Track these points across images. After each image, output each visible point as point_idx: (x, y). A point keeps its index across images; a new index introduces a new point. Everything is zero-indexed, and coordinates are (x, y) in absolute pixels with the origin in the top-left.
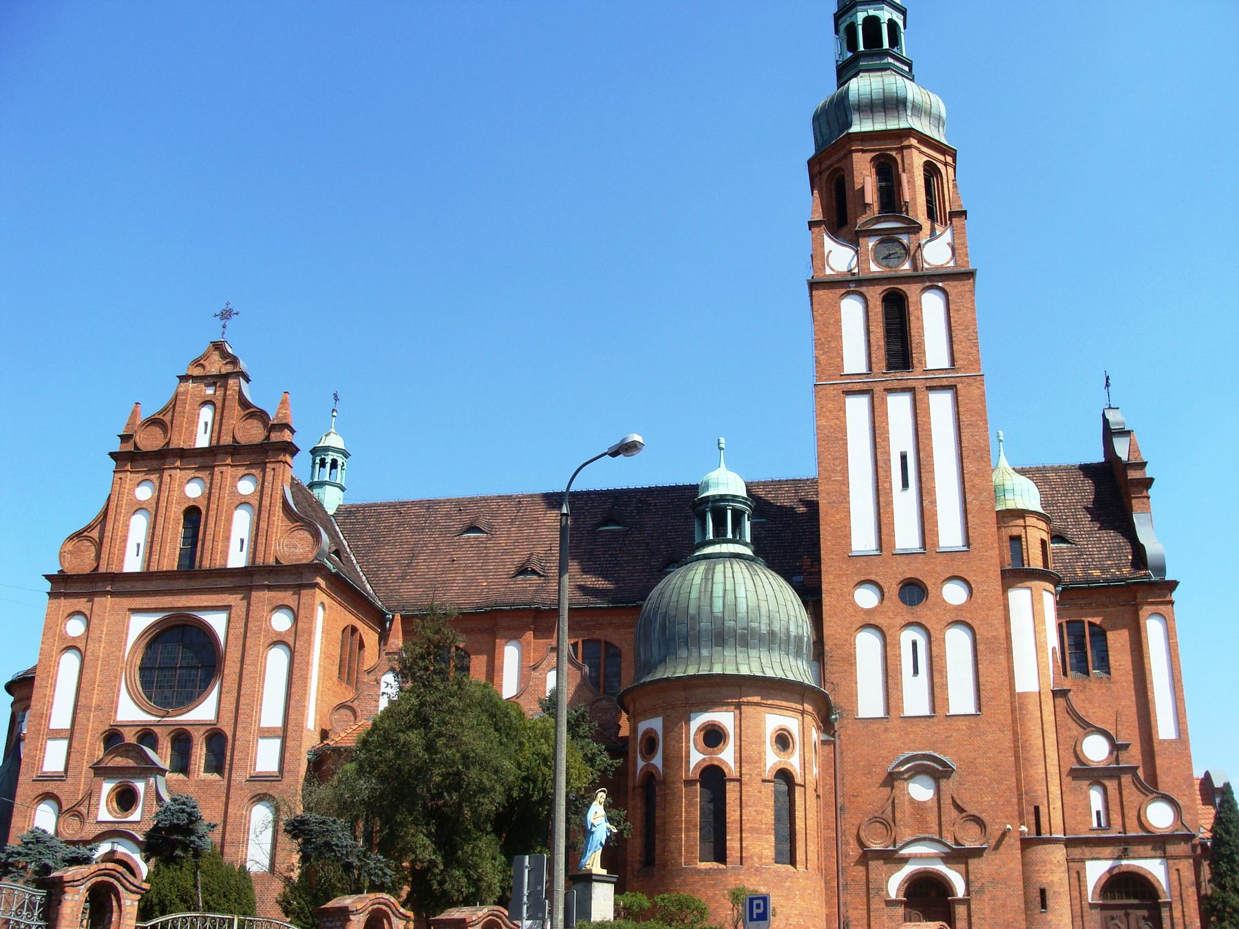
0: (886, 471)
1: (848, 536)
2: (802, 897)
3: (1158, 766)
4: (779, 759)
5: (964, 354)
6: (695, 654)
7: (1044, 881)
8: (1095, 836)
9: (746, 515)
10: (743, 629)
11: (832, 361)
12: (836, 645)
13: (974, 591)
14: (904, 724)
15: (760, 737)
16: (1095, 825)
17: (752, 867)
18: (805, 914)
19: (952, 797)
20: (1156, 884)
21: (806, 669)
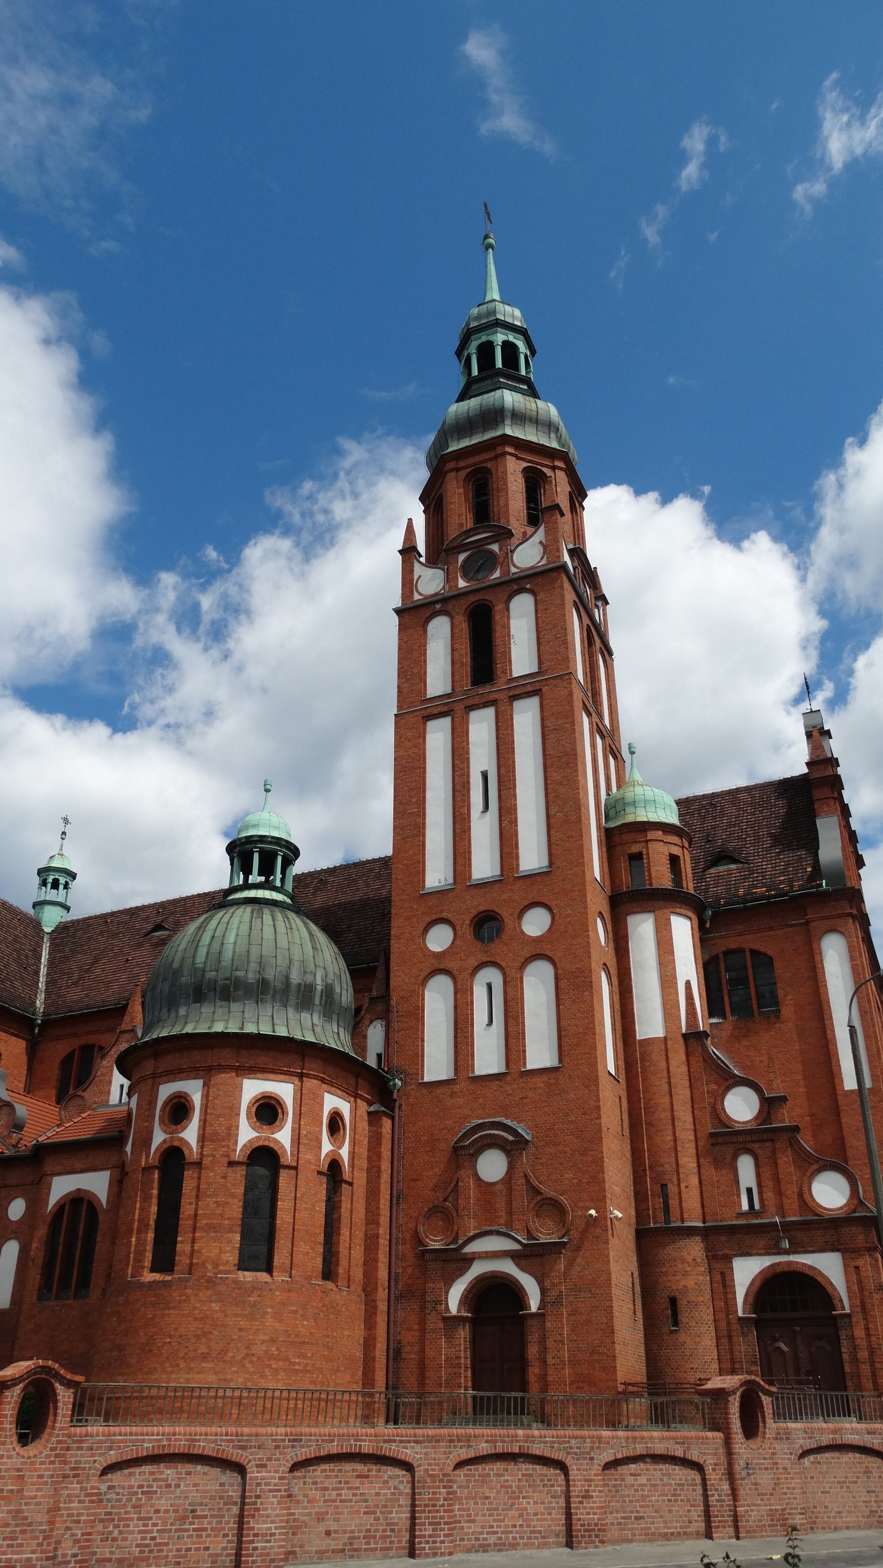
0: (463, 795)
2: (278, 1317)
3: (844, 1126)
5: (551, 654)
6: (173, 1015)
7: (674, 1287)
8: (744, 1222)
9: (279, 859)
11: (414, 688)
12: (402, 998)
16: (745, 1206)
17: (202, 1277)
18: (281, 1339)
19: (526, 1176)
20: (829, 1289)
21: (316, 1021)
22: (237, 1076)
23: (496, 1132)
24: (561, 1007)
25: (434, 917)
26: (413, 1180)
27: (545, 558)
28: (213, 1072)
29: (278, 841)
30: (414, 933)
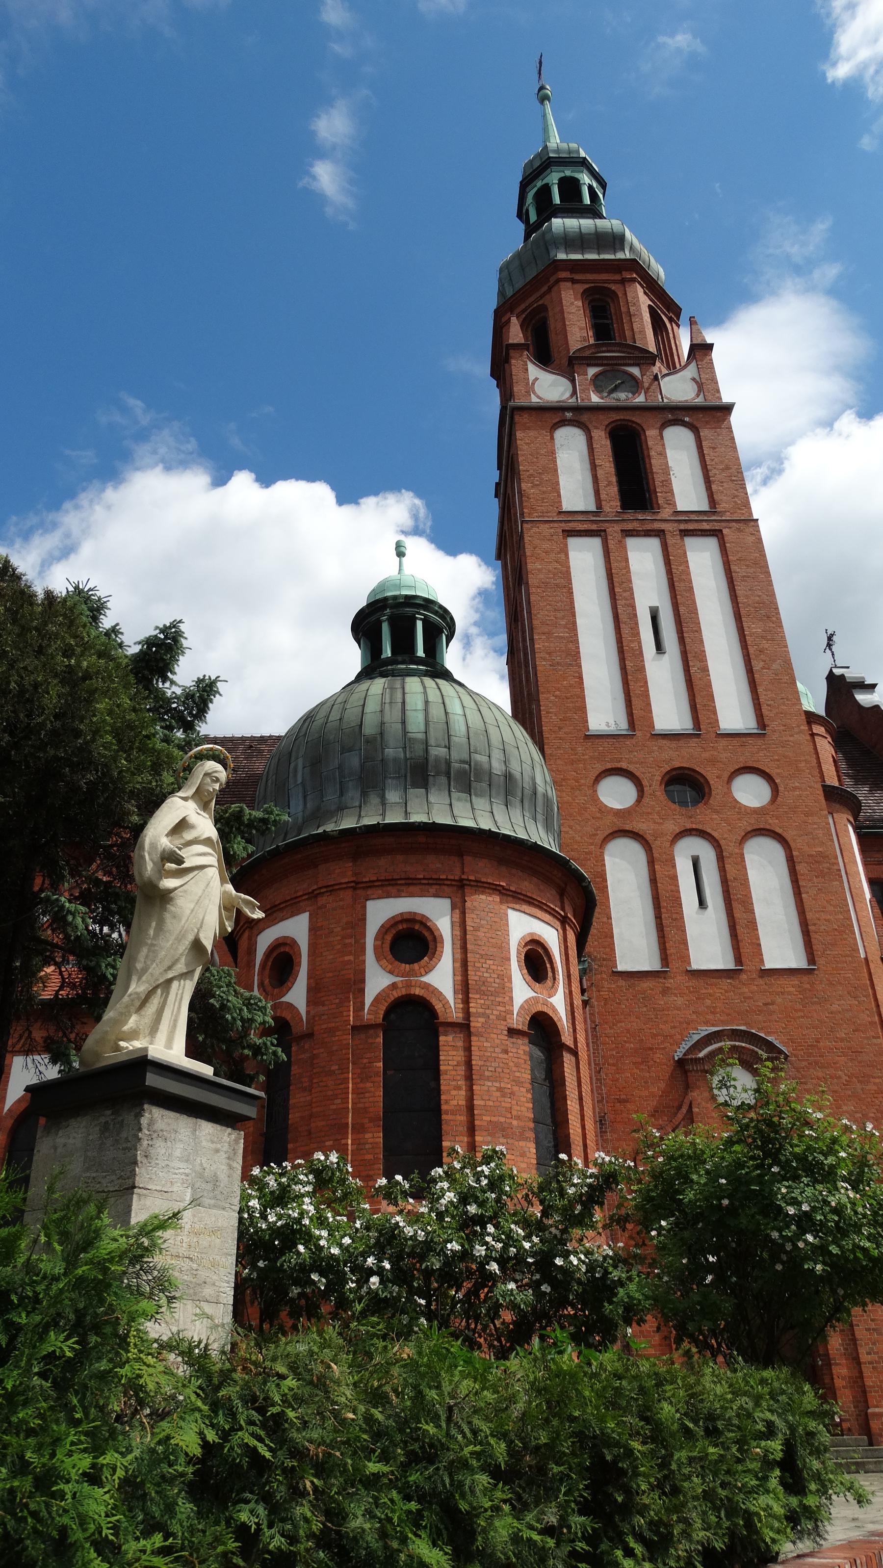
1: (583, 709)
4: (535, 995)
6: (374, 800)
10: (463, 762)
13: (781, 789)
14: (693, 983)
15: (501, 948)
22: (501, 902)
23: (744, 1045)
24: (803, 896)
25: (609, 766)
26: (620, 1101)
27: (702, 395)
28: (467, 890)
29: (444, 613)
30: (583, 781)
